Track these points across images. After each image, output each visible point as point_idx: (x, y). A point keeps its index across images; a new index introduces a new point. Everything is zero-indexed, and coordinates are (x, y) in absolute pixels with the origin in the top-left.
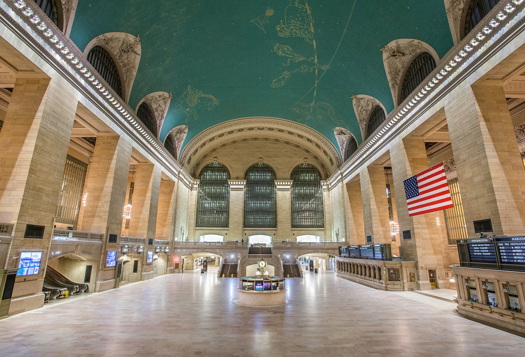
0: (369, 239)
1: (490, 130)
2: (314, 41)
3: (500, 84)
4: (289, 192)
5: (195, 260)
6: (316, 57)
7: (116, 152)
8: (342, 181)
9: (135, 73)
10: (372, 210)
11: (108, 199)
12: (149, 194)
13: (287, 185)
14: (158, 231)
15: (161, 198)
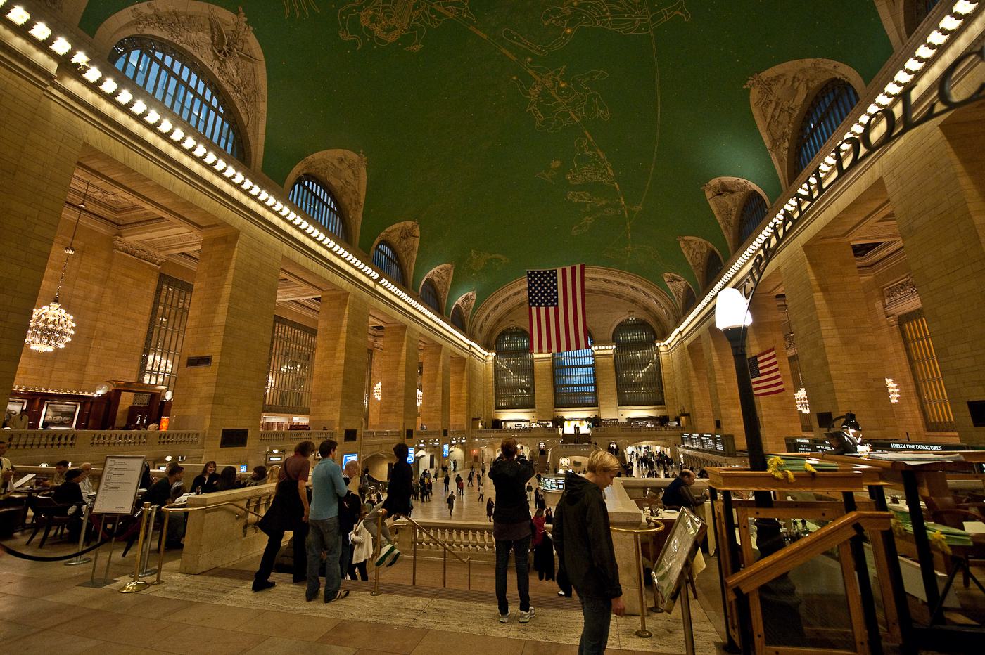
0: (718, 424)
1: (830, 302)
2: (616, 183)
3: (843, 240)
4: (611, 359)
5: (497, 450)
6: (622, 199)
7: (405, 343)
8: (682, 342)
9: (415, 256)
10: (718, 386)
11: (402, 393)
12: (439, 380)
13: (609, 349)
14: (452, 419)
15: (453, 379)
